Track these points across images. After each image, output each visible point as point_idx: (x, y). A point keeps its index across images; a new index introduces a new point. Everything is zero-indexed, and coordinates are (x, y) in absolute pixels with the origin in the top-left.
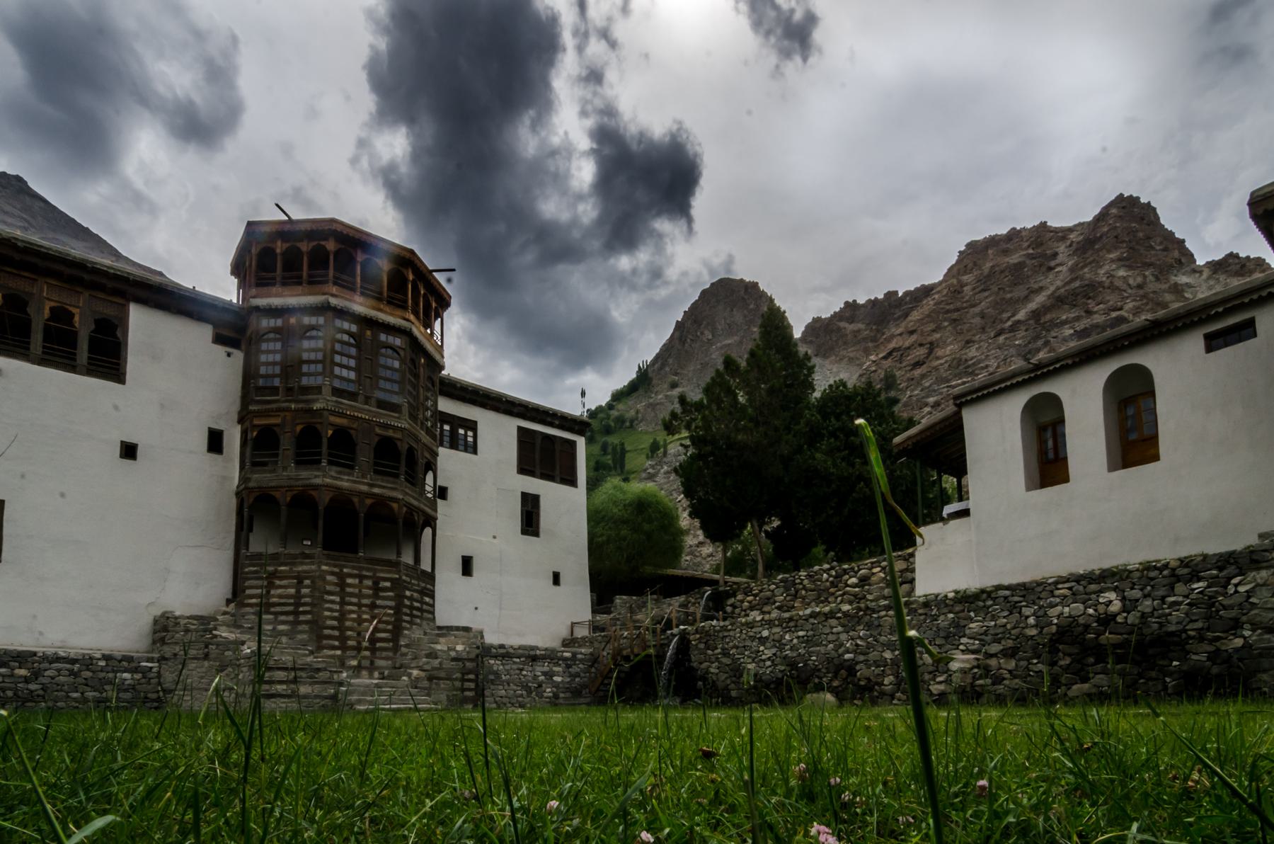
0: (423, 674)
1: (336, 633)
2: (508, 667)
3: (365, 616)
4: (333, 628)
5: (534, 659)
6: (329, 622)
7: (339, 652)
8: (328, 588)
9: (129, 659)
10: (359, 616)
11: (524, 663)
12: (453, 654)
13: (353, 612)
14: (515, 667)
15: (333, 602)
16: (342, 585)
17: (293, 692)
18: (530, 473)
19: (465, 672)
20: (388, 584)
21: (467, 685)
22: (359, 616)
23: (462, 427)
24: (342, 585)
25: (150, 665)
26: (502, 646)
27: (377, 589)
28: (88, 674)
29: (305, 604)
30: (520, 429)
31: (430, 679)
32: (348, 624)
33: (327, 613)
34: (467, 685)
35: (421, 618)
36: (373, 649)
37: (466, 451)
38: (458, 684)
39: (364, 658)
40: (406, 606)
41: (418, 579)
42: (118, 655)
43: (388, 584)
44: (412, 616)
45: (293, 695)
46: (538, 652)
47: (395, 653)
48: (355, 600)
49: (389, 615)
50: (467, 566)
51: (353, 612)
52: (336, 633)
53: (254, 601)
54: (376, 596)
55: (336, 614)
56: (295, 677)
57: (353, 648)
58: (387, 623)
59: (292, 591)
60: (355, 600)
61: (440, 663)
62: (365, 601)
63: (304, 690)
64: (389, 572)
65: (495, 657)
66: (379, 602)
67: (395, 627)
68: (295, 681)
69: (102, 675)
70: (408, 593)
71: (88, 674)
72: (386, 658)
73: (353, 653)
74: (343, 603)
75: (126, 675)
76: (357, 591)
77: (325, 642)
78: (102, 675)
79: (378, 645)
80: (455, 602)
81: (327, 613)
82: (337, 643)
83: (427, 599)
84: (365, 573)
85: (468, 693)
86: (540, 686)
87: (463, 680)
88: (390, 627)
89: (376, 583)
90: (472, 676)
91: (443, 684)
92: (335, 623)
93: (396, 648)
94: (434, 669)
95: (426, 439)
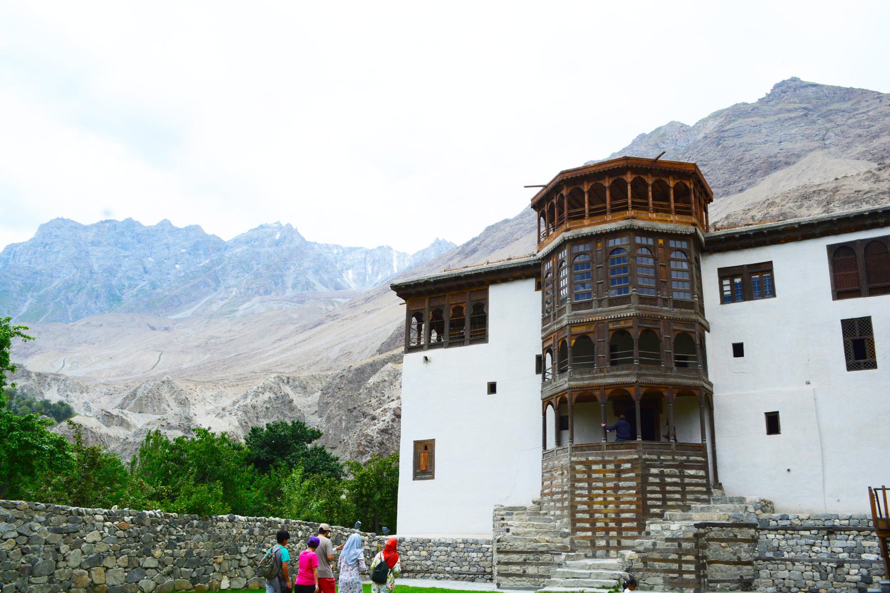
0: (635, 556)
1: (587, 516)
2: (791, 542)
3: (610, 499)
4: (584, 512)
5: (832, 531)
6: (580, 507)
7: (589, 534)
8: (578, 476)
9: (476, 543)
10: (605, 499)
11: (816, 537)
12: (668, 534)
13: (599, 495)
14: (803, 541)
15: (582, 488)
16: (589, 471)
17: (524, 572)
18: (856, 293)
19: (681, 552)
20: (628, 466)
21: (685, 567)
22: (605, 499)
23: (756, 273)
24: (589, 471)
25: (487, 546)
26: (784, 517)
27: (619, 472)
28: (454, 554)
29: (565, 492)
30: (833, 250)
31: (644, 560)
32: (596, 507)
33: (578, 499)
34: (685, 567)
35: (684, 493)
36: (620, 530)
37: (763, 296)
38: (675, 566)
39: (612, 538)
40: (653, 484)
41: (672, 454)
42: (470, 537)
43: (628, 466)
44: (664, 492)
45: (524, 574)
46: (837, 523)
47: (640, 533)
48: (600, 484)
49: (630, 495)
50: (773, 423)
51: (599, 495)
52: (587, 516)
53: (546, 491)
54: (618, 478)
55: (585, 499)
56: (525, 560)
57: (601, 529)
58: (630, 503)
59: (560, 480)
60: (600, 484)
61: (654, 544)
62: (610, 484)
63: (531, 570)
64: (630, 453)
65: (776, 529)
66: (621, 484)
67: (637, 506)
68: (525, 563)
69: (462, 554)
70: (654, 471)
71: (454, 554)
72: (633, 538)
73: (602, 534)
74: (590, 488)
75: (474, 555)
76: (601, 475)
77: (578, 525)
78: (462, 554)
79: (624, 525)
80: (753, 468)
81: (578, 499)
82: (588, 525)
83: (692, 472)
84: (606, 458)
85: (686, 576)
86: (840, 564)
87: (679, 562)
88: (633, 507)
89: (618, 466)
90: (690, 558)
91: (657, 565)
92: (585, 507)
93: (641, 528)
94: (646, 550)
95: (668, 312)
